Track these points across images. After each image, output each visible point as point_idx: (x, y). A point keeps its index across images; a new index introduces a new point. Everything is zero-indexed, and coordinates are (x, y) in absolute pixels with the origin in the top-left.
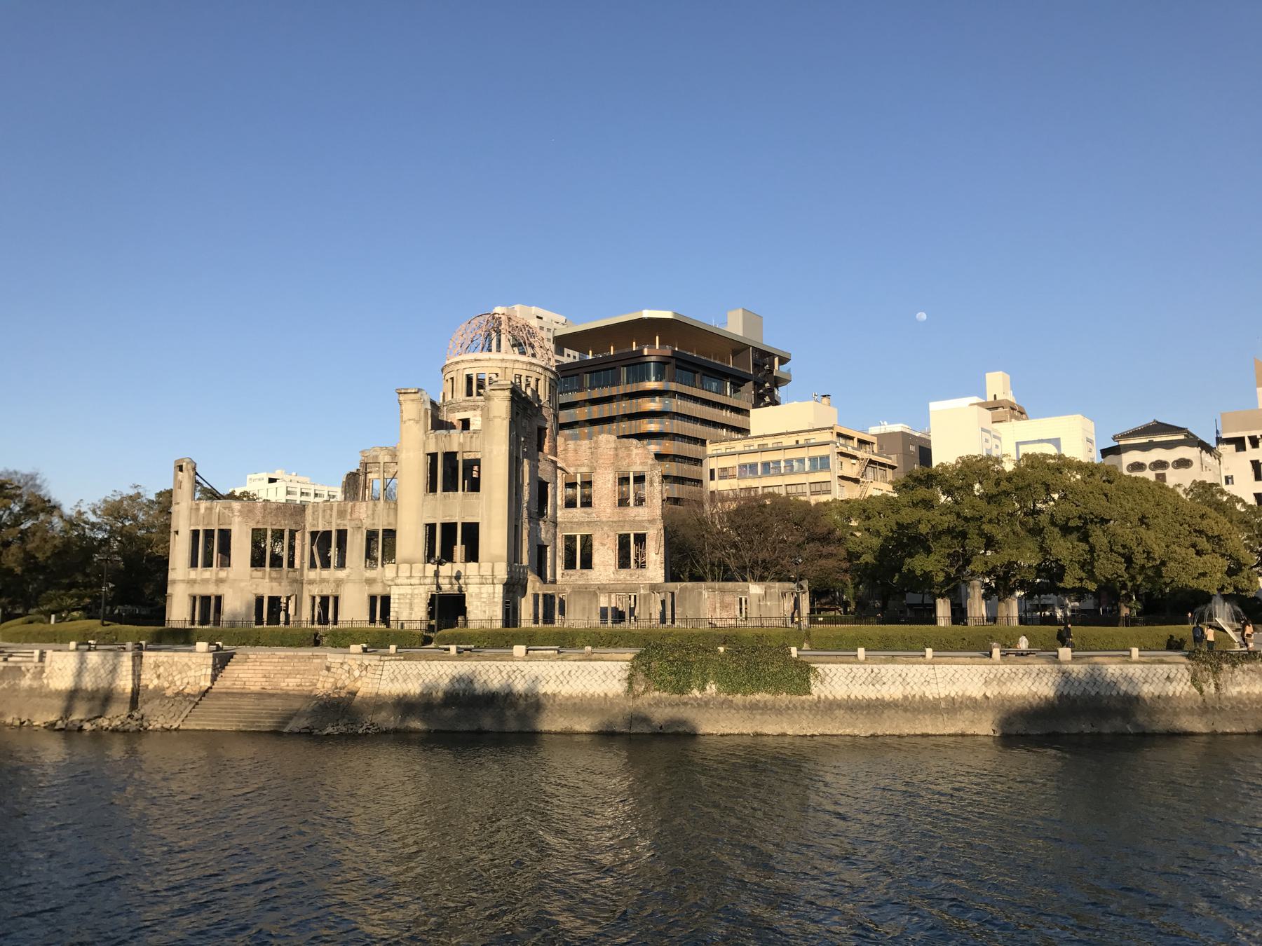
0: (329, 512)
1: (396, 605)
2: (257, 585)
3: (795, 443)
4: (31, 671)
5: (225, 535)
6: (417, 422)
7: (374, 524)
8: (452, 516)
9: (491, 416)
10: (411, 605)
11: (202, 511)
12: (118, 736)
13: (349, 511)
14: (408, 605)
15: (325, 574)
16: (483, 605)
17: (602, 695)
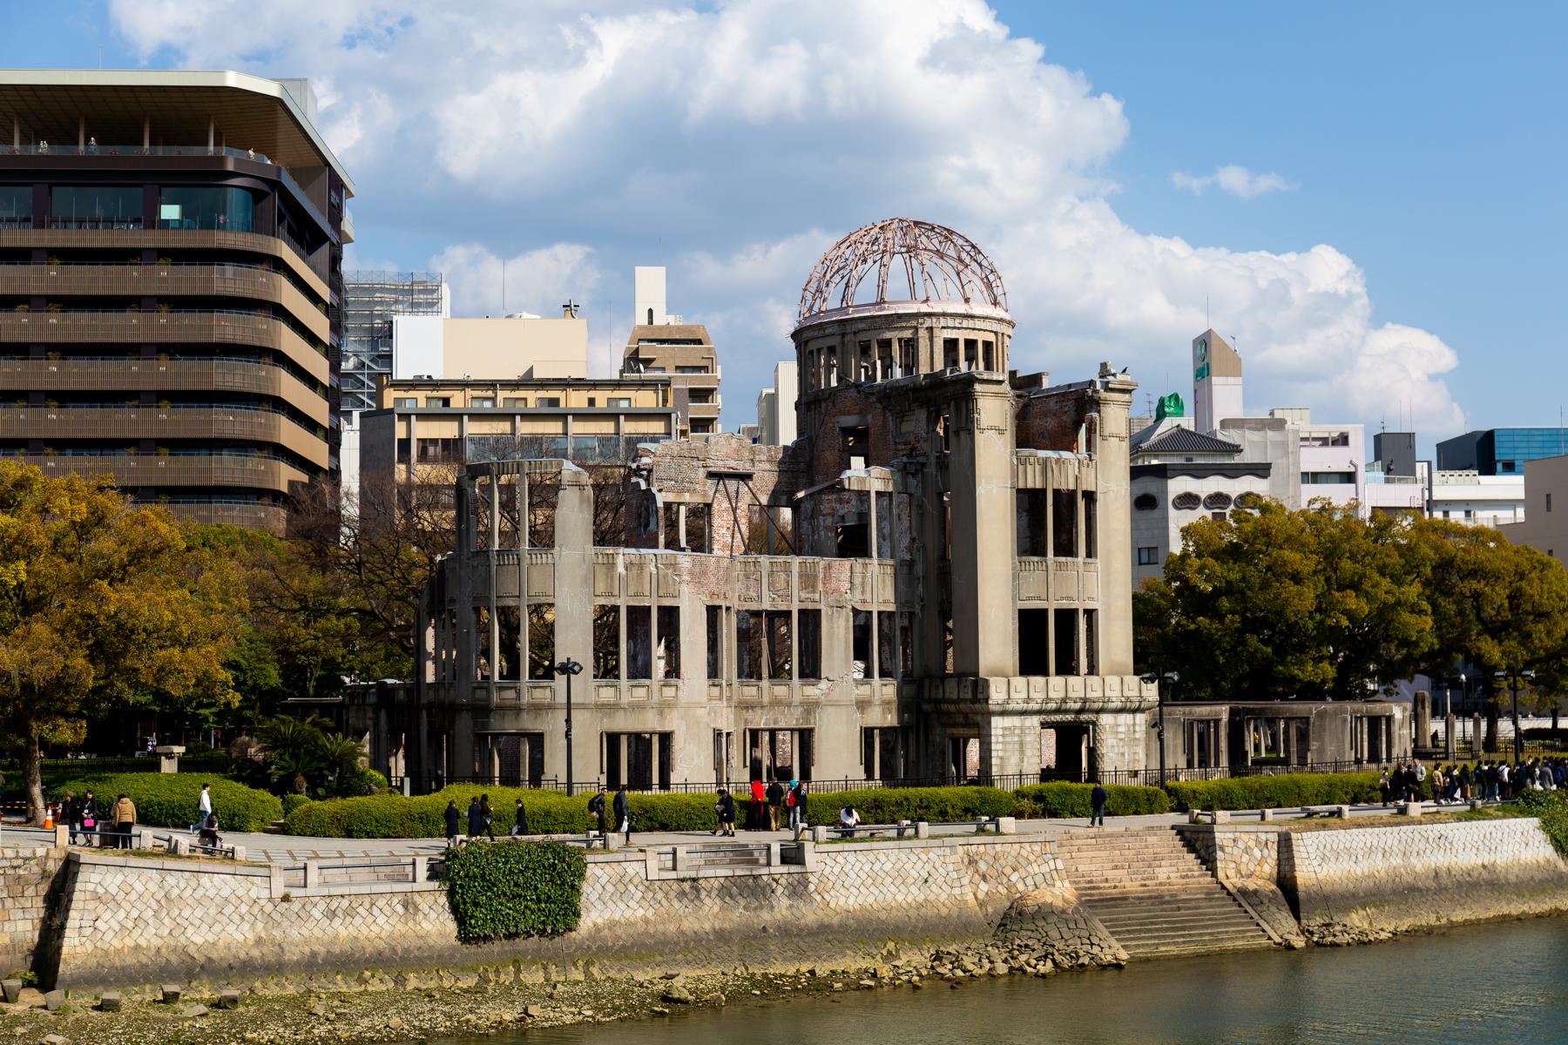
0: (783, 576)
1: (1000, 747)
2: (715, 713)
3: (585, 404)
4: (783, 881)
5: (670, 617)
6: (1001, 432)
7: (864, 601)
8: (1071, 599)
9: (1106, 433)
10: (1021, 744)
11: (621, 569)
12: (1109, 974)
13: (821, 576)
14: (1017, 747)
15: (781, 691)
16: (1121, 743)
17: (1535, 862)
